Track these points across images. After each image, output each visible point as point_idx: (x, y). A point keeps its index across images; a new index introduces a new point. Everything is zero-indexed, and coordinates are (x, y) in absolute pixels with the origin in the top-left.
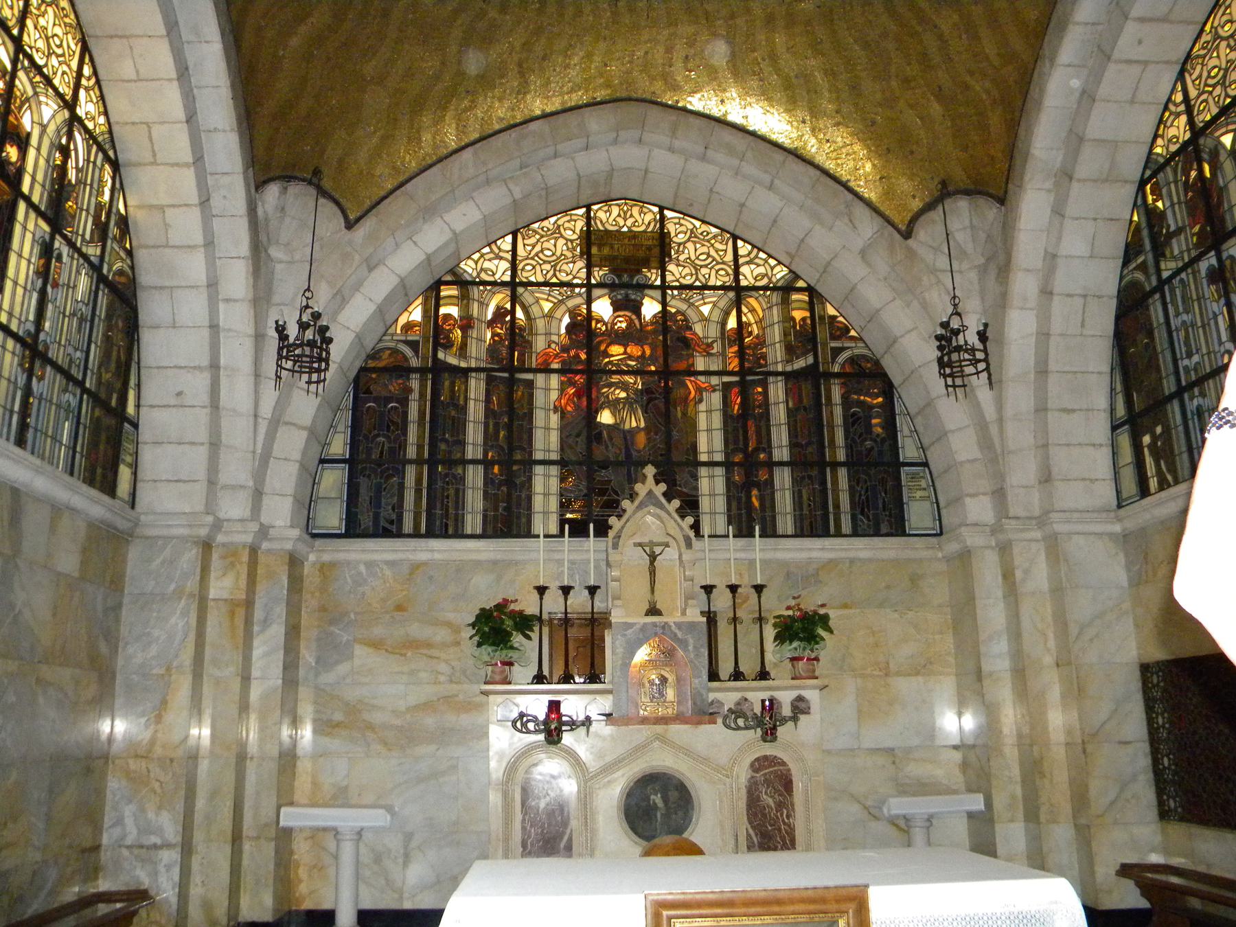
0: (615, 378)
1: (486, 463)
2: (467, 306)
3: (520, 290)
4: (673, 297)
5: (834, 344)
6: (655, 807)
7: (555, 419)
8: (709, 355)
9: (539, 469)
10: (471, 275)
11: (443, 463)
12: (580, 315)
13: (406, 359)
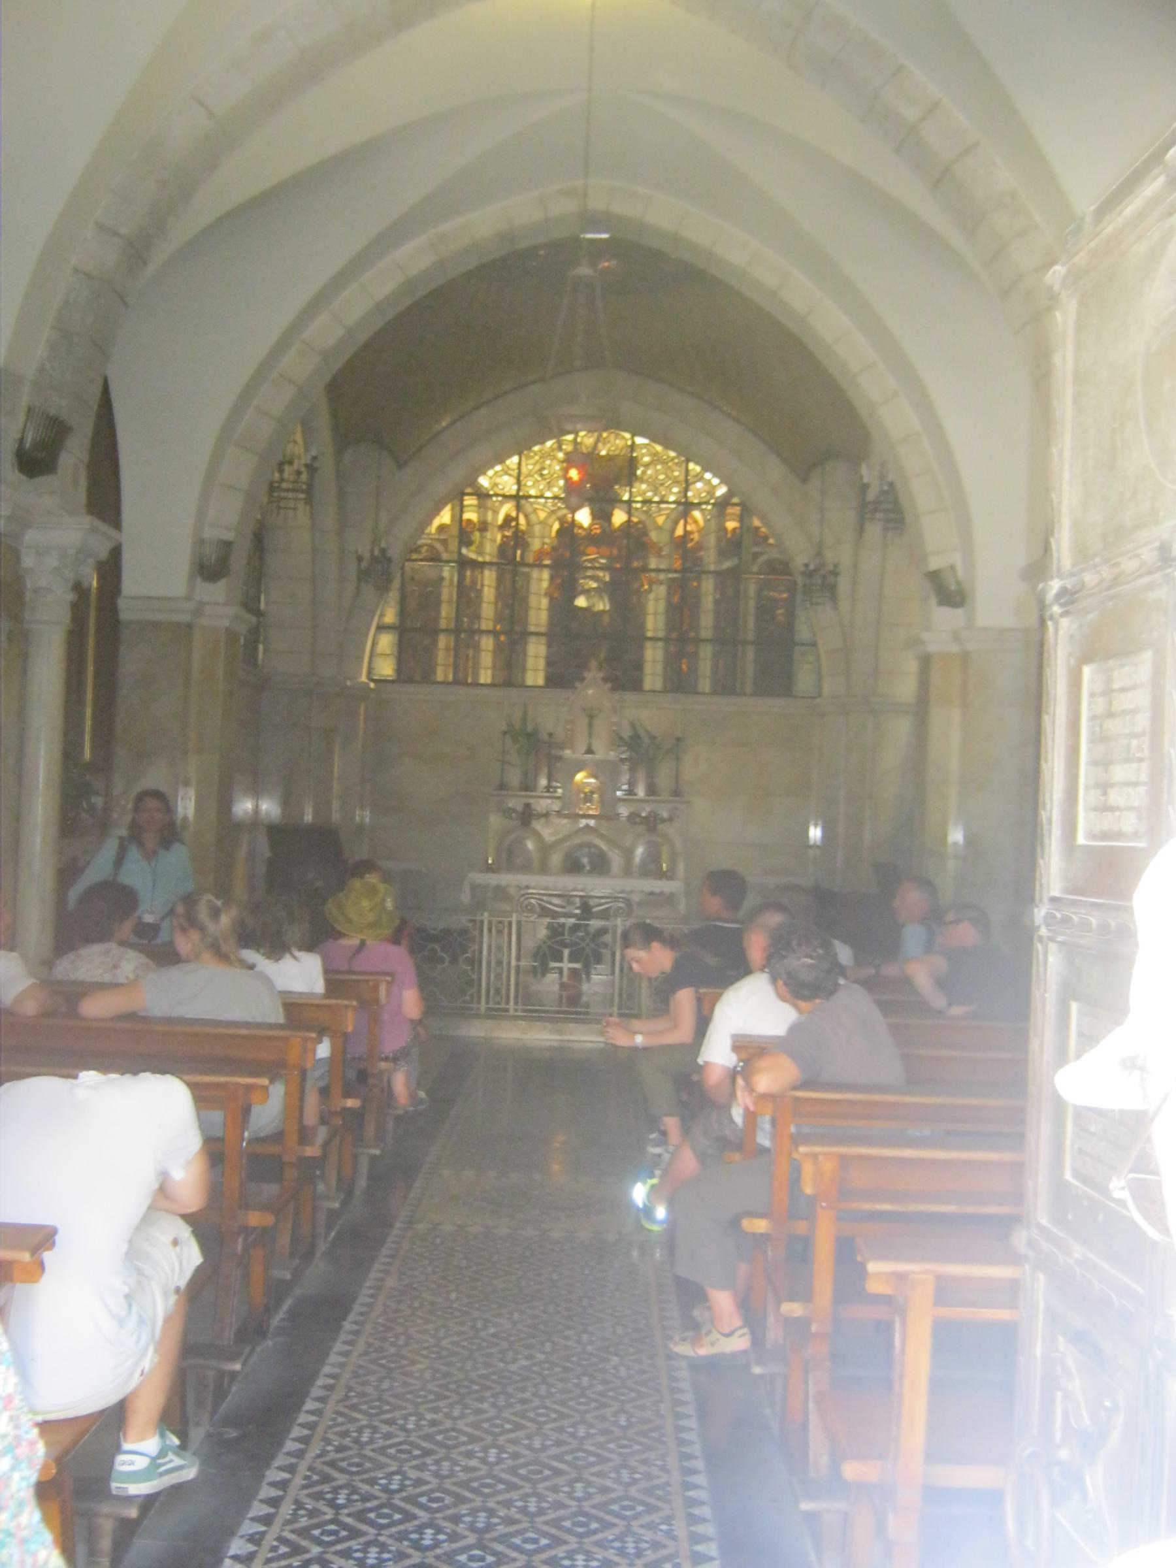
0: (589, 573)
1: (494, 633)
2: (485, 513)
3: (523, 502)
4: (637, 509)
5: (755, 549)
6: (584, 866)
7: (545, 602)
8: (660, 556)
9: (532, 639)
10: (486, 489)
11: (465, 631)
12: (567, 522)
13: (439, 554)
